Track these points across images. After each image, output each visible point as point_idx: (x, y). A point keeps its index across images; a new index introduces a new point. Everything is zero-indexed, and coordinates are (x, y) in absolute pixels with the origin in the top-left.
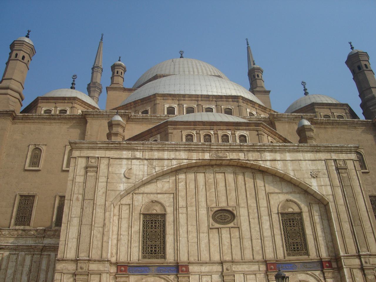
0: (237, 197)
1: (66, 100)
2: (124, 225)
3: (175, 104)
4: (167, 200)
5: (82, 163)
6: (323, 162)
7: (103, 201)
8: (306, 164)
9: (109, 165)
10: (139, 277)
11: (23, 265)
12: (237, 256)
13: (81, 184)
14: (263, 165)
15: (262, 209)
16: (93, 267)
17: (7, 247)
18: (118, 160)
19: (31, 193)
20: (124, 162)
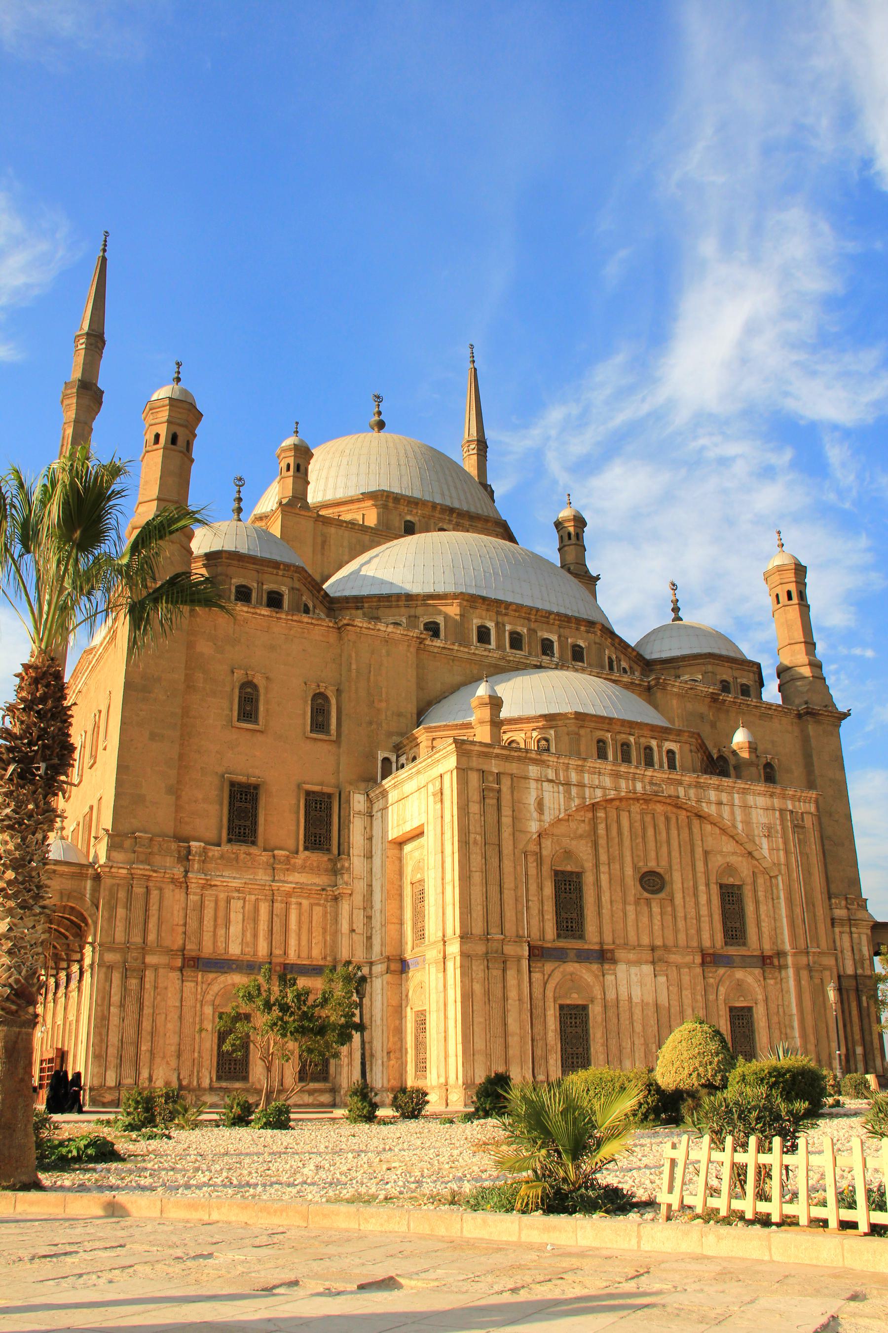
0: (669, 853)
1: (279, 568)
2: (533, 888)
3: (491, 620)
4: (583, 850)
5: (474, 778)
6: (777, 813)
7: (511, 848)
8: (757, 814)
9: (512, 788)
10: (557, 964)
11: (256, 920)
12: (670, 942)
13: (477, 817)
14: (706, 810)
15: (699, 875)
16: (509, 949)
17: (225, 884)
18: (523, 781)
19: (253, 780)
20: (533, 784)
